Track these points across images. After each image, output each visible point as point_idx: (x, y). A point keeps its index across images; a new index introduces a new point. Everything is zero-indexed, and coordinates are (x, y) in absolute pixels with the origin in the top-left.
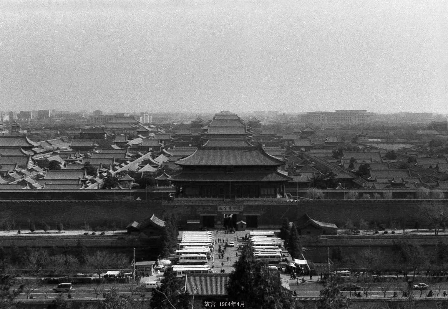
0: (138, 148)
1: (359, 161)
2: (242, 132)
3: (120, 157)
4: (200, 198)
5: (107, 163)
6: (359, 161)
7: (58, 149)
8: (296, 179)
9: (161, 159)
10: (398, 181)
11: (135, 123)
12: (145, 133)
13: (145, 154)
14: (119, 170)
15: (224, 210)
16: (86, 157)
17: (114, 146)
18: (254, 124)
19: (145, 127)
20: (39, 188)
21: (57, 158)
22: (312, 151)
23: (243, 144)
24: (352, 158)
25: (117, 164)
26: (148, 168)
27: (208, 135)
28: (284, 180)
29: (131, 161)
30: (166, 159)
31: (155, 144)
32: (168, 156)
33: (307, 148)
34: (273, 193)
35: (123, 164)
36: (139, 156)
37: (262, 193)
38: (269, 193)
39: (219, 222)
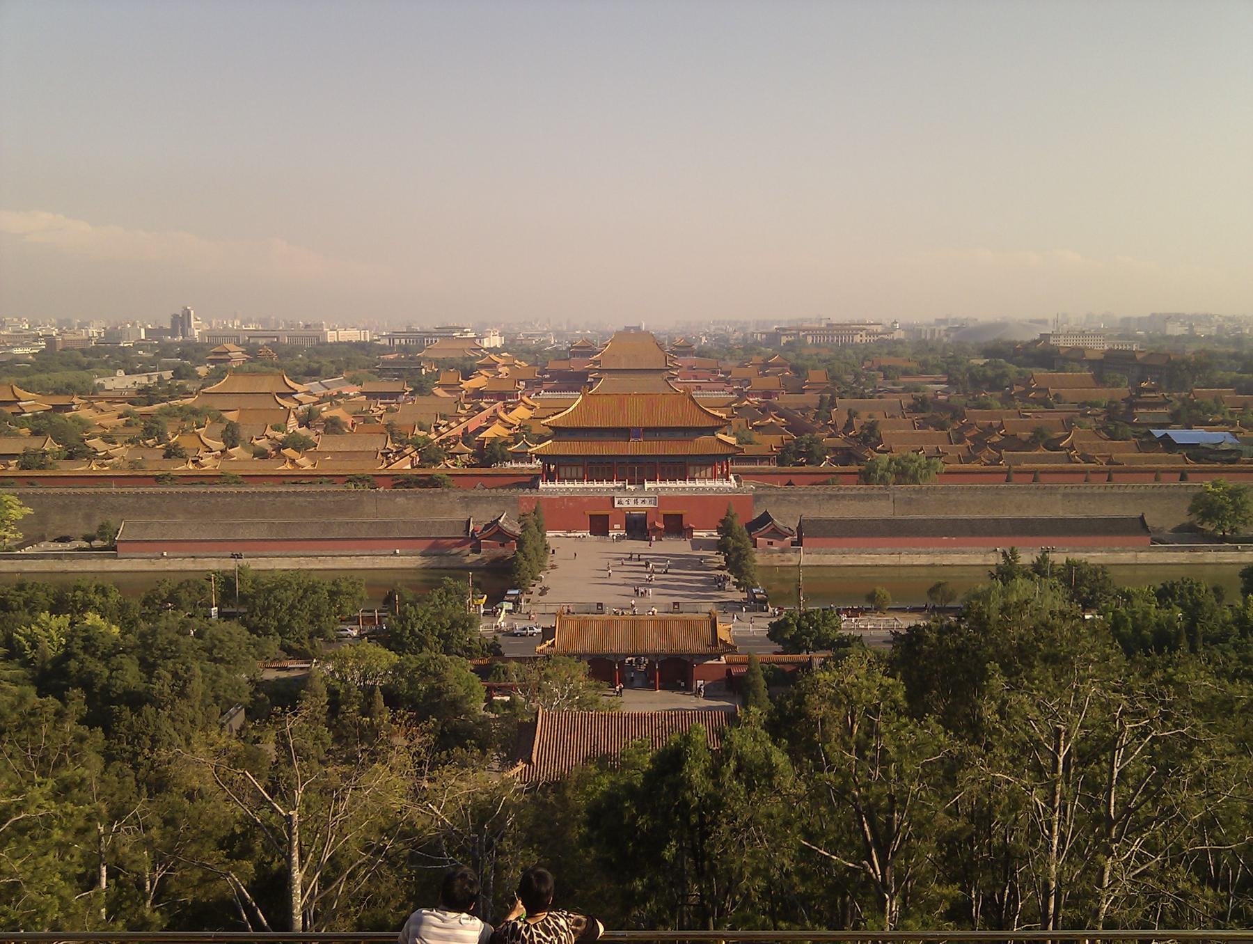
0: (478, 393)
3: (448, 411)
4: (586, 484)
7: (340, 395)
9: (521, 413)
11: (475, 350)
12: (492, 366)
15: (625, 505)
17: (439, 392)
19: (492, 356)
20: (309, 467)
21: (338, 413)
25: (444, 422)
26: (495, 431)
28: (731, 451)
30: (529, 414)
35: (453, 424)
39: (616, 526)
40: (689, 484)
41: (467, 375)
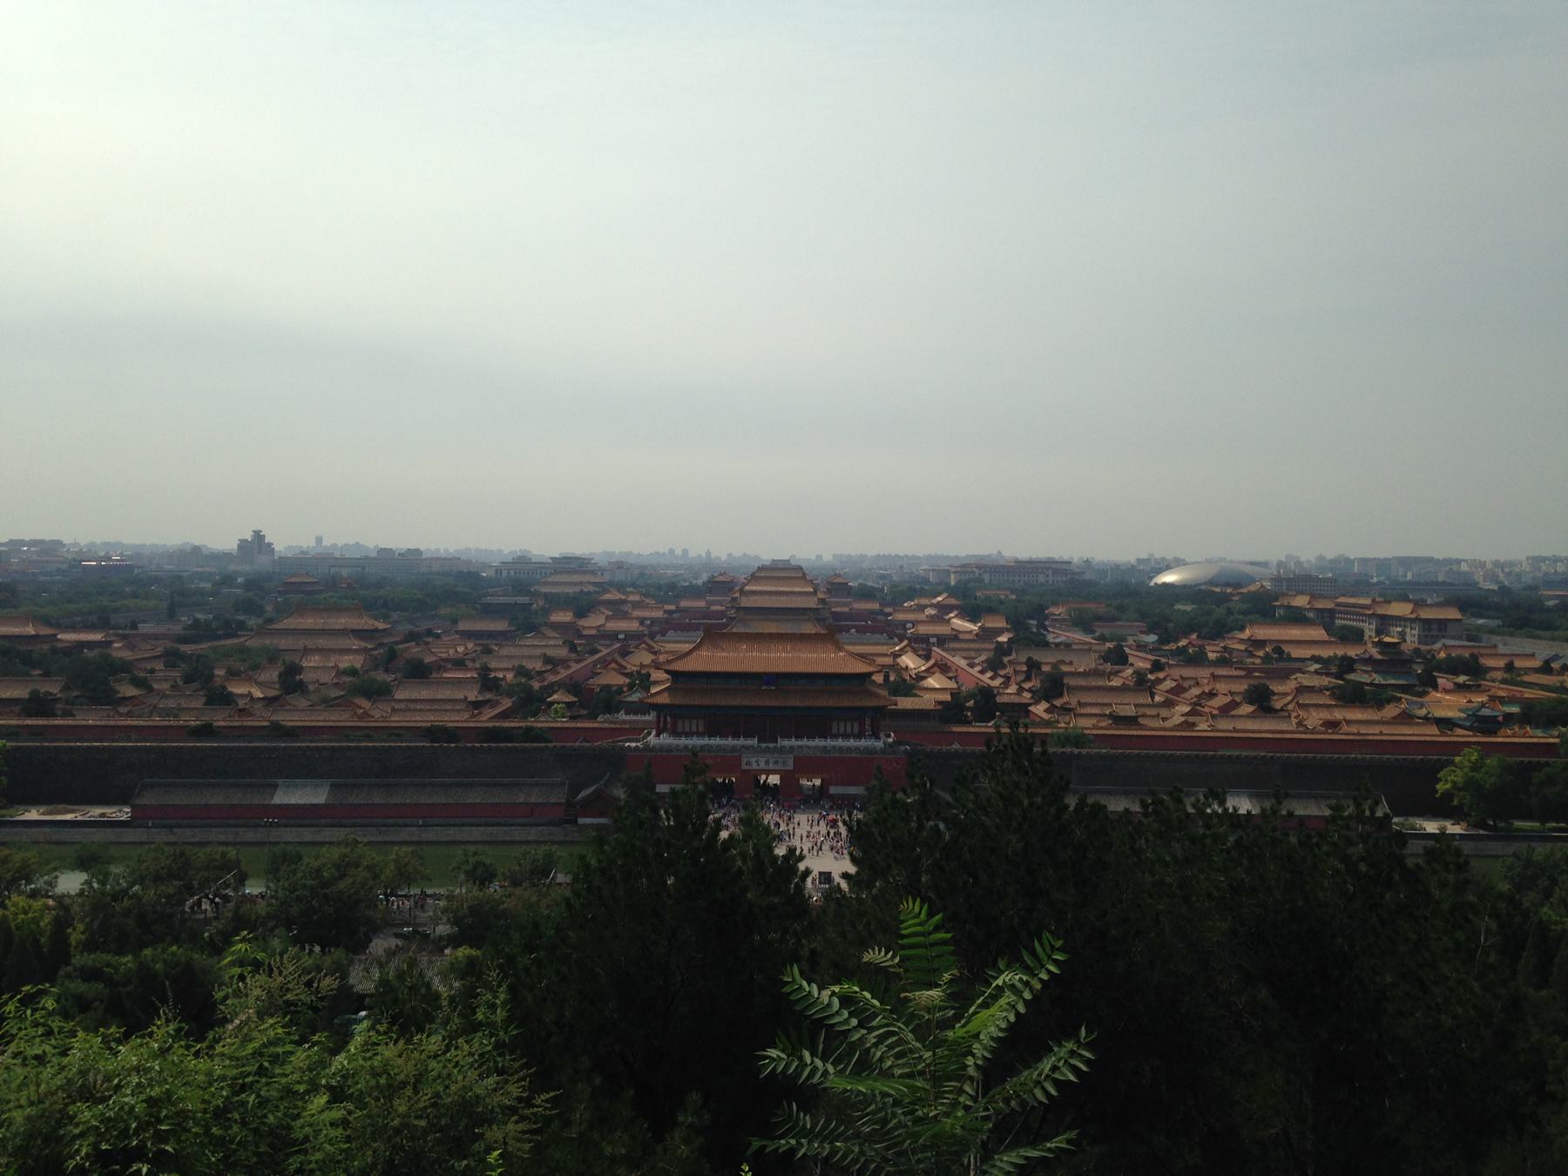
1: (1045, 668)
2: (811, 603)
5: (529, 665)
6: (1045, 668)
8: (905, 703)
10: (1129, 711)
13: (607, 646)
14: (552, 678)
16: (487, 651)
18: (837, 586)
22: (952, 645)
23: (809, 628)
24: (1030, 659)
27: (739, 609)
29: (578, 661)
31: (634, 626)
32: (655, 653)
33: (942, 641)
34: (856, 730)
36: (594, 652)
37: (835, 731)
38: (849, 730)
40: (830, 743)
41: (581, 613)
